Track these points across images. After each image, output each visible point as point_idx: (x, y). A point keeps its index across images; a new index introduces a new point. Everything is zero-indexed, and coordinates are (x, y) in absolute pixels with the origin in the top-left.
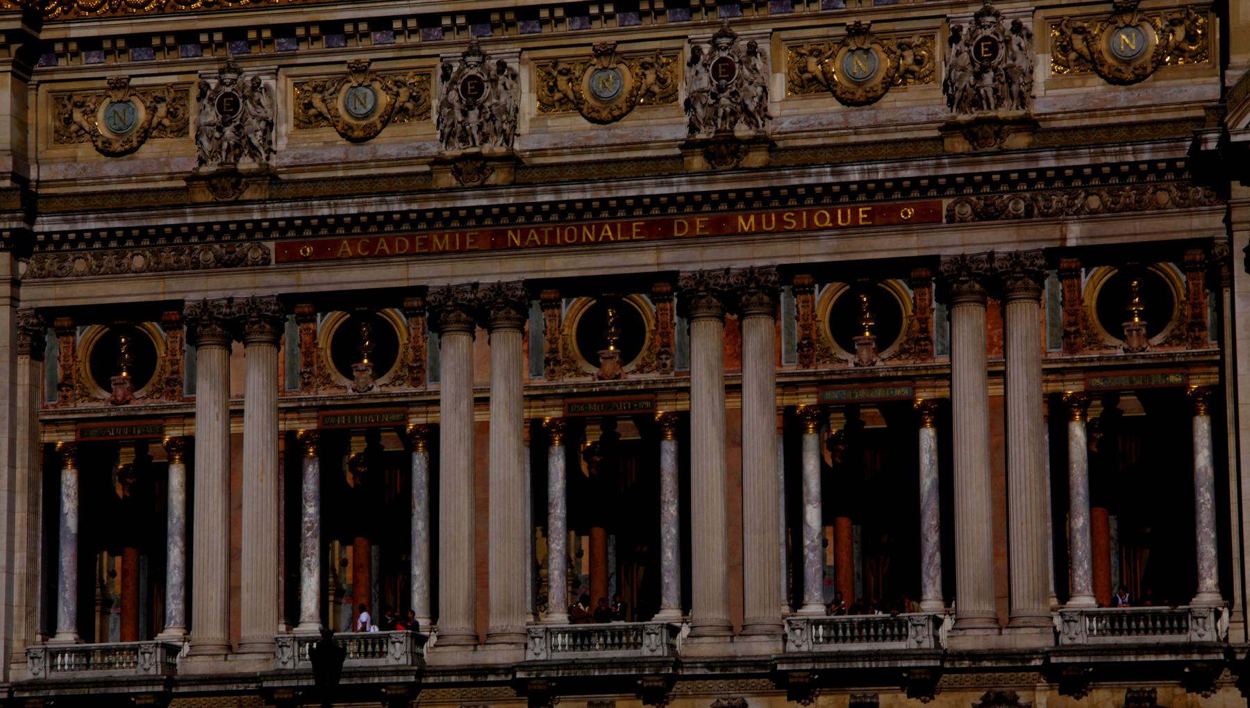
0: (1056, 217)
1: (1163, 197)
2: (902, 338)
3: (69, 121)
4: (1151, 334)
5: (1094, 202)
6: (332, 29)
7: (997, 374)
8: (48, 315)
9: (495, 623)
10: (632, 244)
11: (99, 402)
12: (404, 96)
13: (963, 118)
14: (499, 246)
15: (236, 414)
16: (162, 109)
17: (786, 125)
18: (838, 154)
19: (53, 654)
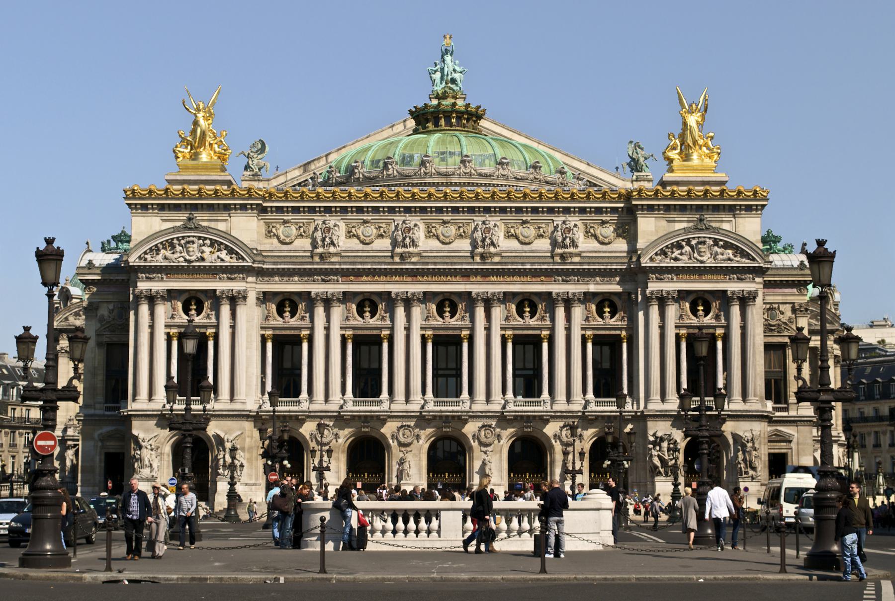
2: (537, 315)
3: (270, 232)
5: (598, 279)
6: (360, 210)
8: (264, 293)
10: (458, 283)
16: (302, 230)
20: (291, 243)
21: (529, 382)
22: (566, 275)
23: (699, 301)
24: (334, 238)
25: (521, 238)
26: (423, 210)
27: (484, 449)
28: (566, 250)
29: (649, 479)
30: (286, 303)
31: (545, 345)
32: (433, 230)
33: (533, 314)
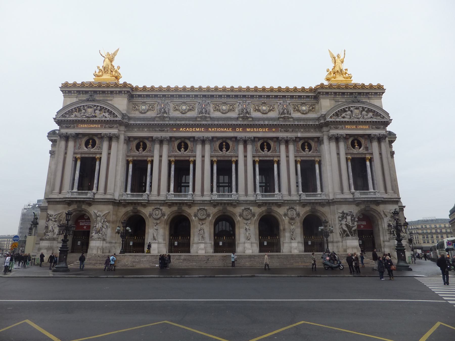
0: (296, 132)
1: (312, 130)
3: (135, 108)
4: (309, 151)
5: (302, 130)
6: (180, 96)
7: (287, 156)
8: (129, 138)
9: (205, 193)
11: (137, 153)
12: (191, 107)
13: (282, 116)
14: (207, 131)
15: (161, 156)
16: (151, 107)
17: (253, 116)
18: (264, 119)
19: (127, 194)
20: (145, 113)
21: (268, 185)
22: (286, 128)
23: (356, 141)
24: (166, 109)
25: (262, 111)
26: (212, 96)
27: (246, 222)
28: (285, 115)
29: (340, 239)
30: (142, 144)
31: (275, 166)
32: (217, 107)
33: (269, 149)
